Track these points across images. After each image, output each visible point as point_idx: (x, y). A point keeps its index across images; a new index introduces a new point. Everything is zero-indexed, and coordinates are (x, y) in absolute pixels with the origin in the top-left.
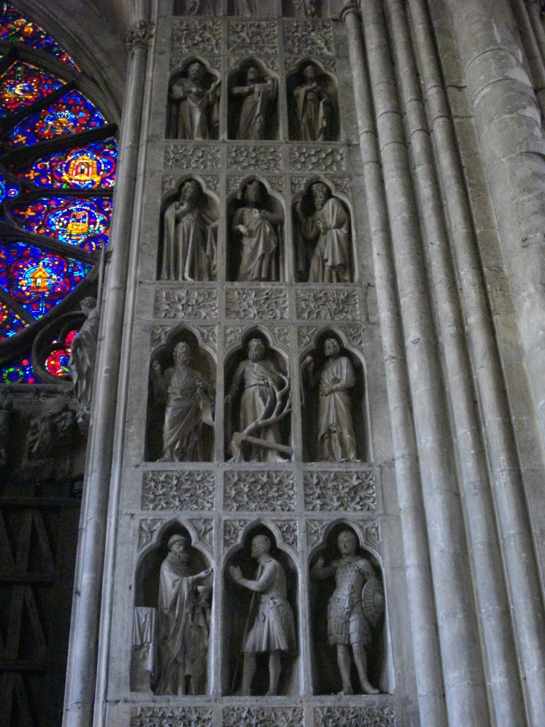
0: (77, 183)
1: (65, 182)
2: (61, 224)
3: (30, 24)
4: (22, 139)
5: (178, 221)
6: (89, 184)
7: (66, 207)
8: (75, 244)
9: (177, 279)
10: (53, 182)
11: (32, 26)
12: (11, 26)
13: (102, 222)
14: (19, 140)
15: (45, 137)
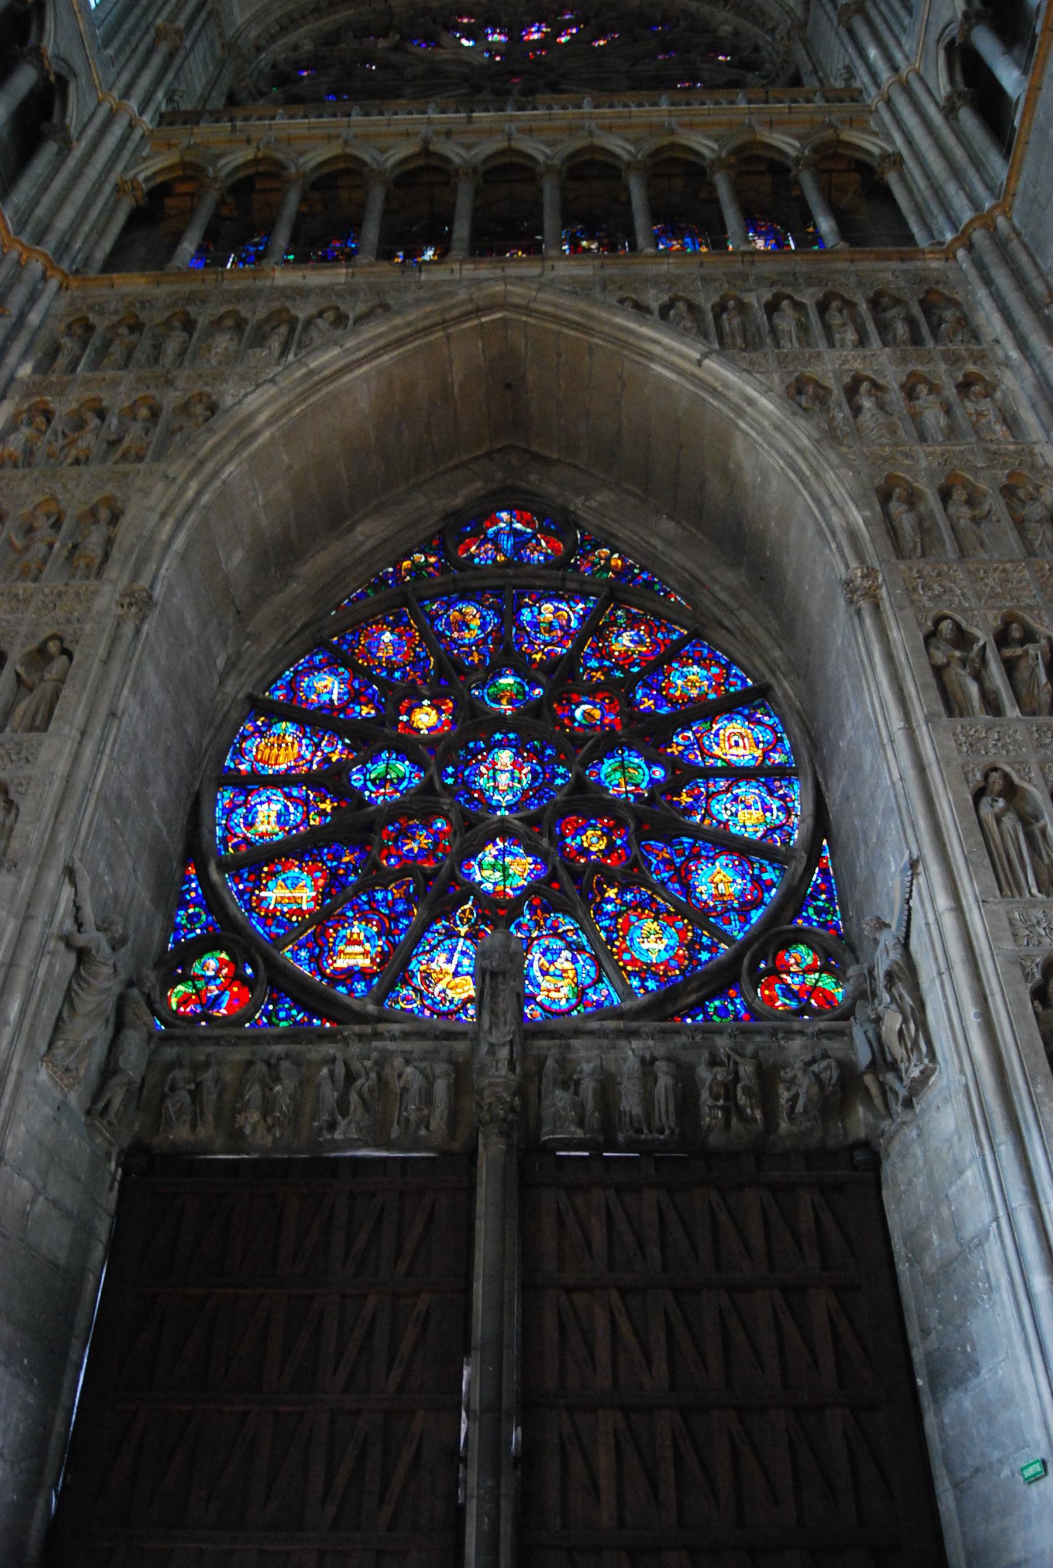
0: (734, 758)
1: (718, 757)
3: (616, 556)
4: (649, 703)
5: (998, 821)
7: (728, 790)
9: (1021, 895)
10: (703, 759)
12: (591, 558)
13: (778, 809)
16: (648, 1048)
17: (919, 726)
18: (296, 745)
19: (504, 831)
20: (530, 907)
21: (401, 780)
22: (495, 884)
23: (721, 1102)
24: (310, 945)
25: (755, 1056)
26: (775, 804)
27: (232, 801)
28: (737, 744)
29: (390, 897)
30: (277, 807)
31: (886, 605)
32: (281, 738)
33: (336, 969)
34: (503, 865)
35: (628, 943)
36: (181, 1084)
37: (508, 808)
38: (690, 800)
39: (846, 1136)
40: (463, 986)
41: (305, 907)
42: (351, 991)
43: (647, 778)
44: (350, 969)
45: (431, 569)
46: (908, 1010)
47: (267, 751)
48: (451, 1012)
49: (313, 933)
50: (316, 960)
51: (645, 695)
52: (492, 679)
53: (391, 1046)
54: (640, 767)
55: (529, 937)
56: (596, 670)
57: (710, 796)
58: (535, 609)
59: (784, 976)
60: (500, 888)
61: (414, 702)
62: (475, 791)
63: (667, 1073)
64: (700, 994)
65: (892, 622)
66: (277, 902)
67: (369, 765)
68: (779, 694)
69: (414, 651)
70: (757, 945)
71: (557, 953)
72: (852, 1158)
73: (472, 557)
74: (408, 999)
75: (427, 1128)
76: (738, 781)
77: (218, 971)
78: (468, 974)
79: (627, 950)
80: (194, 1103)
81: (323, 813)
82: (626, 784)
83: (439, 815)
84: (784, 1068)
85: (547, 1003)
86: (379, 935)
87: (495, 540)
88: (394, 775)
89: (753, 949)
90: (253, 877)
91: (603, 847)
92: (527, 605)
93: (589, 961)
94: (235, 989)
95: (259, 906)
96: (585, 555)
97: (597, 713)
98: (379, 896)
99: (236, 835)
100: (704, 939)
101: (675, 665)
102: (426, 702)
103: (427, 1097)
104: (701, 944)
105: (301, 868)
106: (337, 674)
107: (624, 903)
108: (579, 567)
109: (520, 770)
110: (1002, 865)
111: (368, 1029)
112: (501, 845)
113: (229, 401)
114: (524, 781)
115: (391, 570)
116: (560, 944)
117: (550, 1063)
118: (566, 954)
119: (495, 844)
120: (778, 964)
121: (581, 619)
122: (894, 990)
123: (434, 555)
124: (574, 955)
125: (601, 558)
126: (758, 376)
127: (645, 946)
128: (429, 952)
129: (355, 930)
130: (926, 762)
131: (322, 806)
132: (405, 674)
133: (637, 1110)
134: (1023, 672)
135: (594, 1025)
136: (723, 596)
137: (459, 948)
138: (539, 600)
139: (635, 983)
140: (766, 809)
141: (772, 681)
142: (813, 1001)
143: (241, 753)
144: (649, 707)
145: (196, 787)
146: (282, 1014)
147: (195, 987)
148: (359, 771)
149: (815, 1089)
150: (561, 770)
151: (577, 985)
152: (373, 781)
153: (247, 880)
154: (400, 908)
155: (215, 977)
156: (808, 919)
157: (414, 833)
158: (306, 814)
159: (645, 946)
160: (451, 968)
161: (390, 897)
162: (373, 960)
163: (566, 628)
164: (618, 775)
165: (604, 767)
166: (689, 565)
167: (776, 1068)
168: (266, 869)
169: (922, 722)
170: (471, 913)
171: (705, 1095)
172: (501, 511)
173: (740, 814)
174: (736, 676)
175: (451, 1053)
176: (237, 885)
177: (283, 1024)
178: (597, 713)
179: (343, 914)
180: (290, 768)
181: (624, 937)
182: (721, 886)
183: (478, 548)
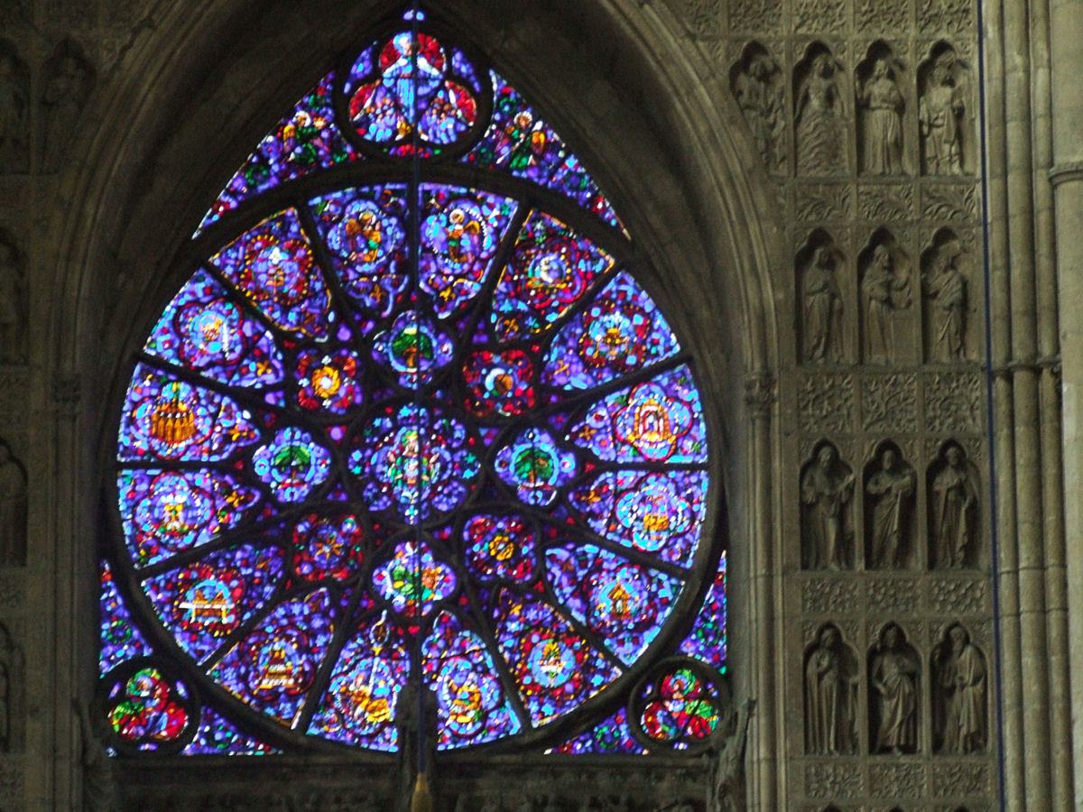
1: (632, 445)
2: (635, 516)
3: (539, 125)
5: (820, 677)
7: (636, 488)
11: (543, 130)
17: (777, 575)
19: (412, 536)
25: (630, 803)
31: (776, 422)
32: (173, 405)
33: (262, 690)
40: (380, 710)
47: (161, 422)
49: (238, 651)
57: (618, 495)
58: (443, 217)
65: (777, 455)
66: (197, 616)
73: (366, 122)
74: (330, 723)
77: (153, 690)
79: (529, 672)
81: (230, 508)
86: (300, 651)
92: (436, 213)
98: (296, 609)
102: (326, 360)
105: (217, 577)
107: (527, 622)
109: (430, 456)
110: (813, 724)
113: (105, 61)
118: (472, 675)
122: (726, 800)
126: (701, 44)
128: (346, 673)
129: (277, 647)
130: (776, 615)
134: (881, 512)
136: (655, 220)
137: (374, 670)
141: (696, 356)
147: (132, 708)
150: (471, 459)
152: (278, 467)
153: (165, 588)
154: (317, 623)
155: (151, 698)
159: (545, 669)
160: (368, 690)
169: (780, 572)
170: (384, 631)
173: (646, 518)
178: (509, 380)
182: (619, 604)
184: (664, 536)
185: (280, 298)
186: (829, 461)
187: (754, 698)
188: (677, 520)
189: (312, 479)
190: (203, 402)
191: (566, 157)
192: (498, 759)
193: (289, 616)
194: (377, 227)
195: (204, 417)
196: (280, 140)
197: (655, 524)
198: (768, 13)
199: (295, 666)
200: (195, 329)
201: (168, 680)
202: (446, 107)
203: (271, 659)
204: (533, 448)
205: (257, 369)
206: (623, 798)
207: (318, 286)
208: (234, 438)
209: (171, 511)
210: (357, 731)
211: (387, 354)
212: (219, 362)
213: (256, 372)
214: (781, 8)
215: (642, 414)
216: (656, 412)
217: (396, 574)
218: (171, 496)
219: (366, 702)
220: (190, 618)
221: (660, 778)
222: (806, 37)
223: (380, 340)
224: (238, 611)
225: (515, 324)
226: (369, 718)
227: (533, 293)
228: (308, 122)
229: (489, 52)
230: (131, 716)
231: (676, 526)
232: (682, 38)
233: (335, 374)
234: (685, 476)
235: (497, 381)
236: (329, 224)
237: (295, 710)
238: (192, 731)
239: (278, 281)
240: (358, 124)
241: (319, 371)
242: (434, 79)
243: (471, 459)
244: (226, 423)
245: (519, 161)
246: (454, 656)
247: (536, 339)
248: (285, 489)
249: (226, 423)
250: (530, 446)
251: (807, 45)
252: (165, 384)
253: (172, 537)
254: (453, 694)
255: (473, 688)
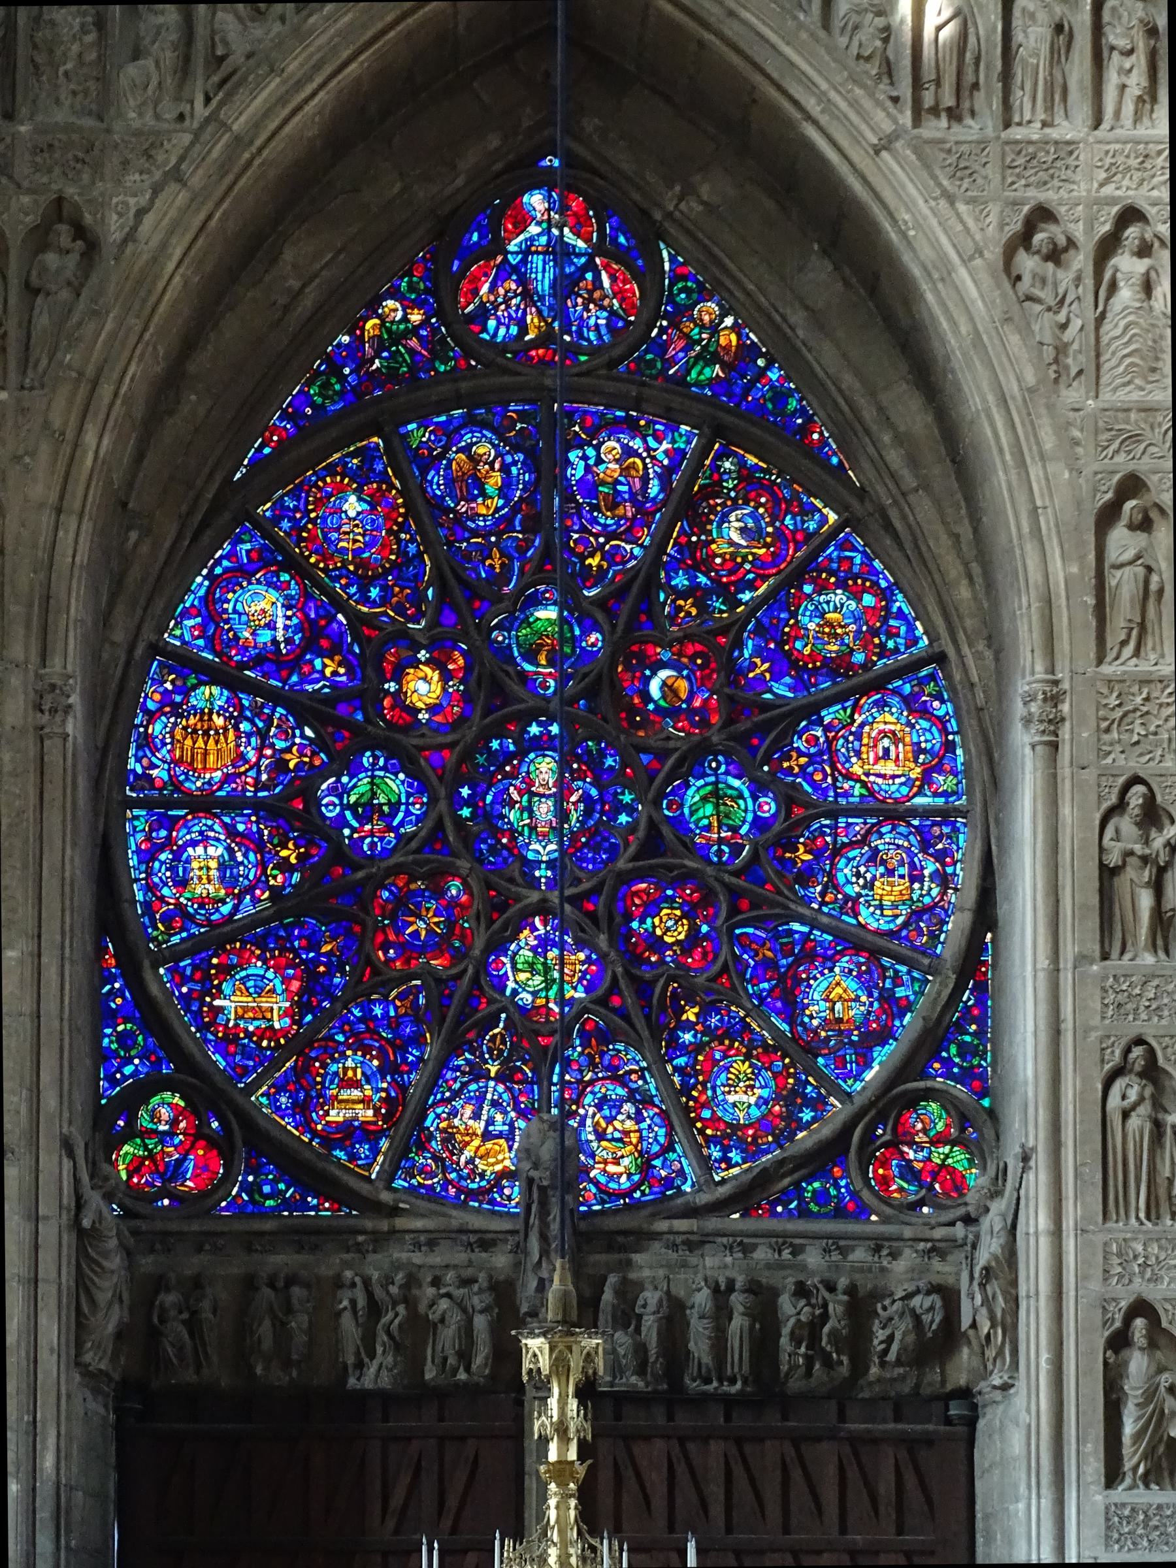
1: (858, 780)
2: (861, 881)
3: (729, 321)
5: (1126, 1115)
6: (902, 784)
7: (864, 841)
8: (892, 926)
10: (835, 780)
11: (735, 328)
13: (932, 877)
14: (758, 671)
15: (806, 664)
16: (725, 1267)
18: (231, 735)
19: (543, 909)
20: (583, 1034)
21: (395, 807)
22: (535, 994)
23: (803, 1350)
24: (291, 1087)
25: (852, 1290)
26: (930, 867)
27: (149, 838)
28: (886, 751)
29: (392, 1013)
30: (217, 851)
34: (545, 964)
35: (709, 1093)
36: (173, 1313)
37: (551, 864)
38: (808, 857)
39: (943, 1382)
41: (277, 1026)
42: (353, 1157)
43: (750, 817)
44: (348, 1123)
45: (414, 343)
46: (999, 1315)
47: (189, 742)
48: (482, 1191)
49: (293, 1068)
50: (303, 1110)
51: (758, 652)
52: (522, 610)
53: (417, 1258)
54: (741, 796)
55: (580, 1081)
56: (683, 594)
57: (838, 851)
59: (906, 1149)
60: (540, 1002)
61: (405, 653)
62: (503, 833)
63: (744, 1314)
64: (796, 1176)
67: (345, 779)
68: (958, 677)
69: (399, 541)
70: (873, 1112)
71: (617, 1105)
72: (947, 1409)
73: (483, 313)
74: (424, 1171)
75: (468, 1369)
76: (880, 824)
77: (174, 1123)
78: (500, 1135)
80: (192, 1335)
81: (285, 866)
82: (720, 827)
83: (455, 875)
84: (883, 1297)
85: (602, 1180)
86: (382, 1071)
87: (520, 273)
88: (383, 801)
89: (866, 1119)
90: (198, 975)
91: (682, 937)
92: (581, 445)
93: (657, 1120)
94: (201, 1152)
95: (213, 1023)
96: (675, 324)
97: (683, 686)
98: (378, 1011)
99: (162, 899)
100: (809, 1089)
101: (808, 589)
102: (423, 655)
103: (467, 1329)
104: (804, 1096)
106: (280, 587)
107: (707, 1031)
108: (665, 346)
111: (384, 1225)
112: (542, 931)
113: (114, 228)
114: (574, 816)
115: (346, 339)
116: (621, 1091)
117: (608, 1296)
118: (628, 1107)
119: (534, 929)
120: (900, 1129)
121: (665, 477)
122: (988, 1287)
123: (418, 304)
124: (638, 1112)
125: (703, 327)
126: (962, 207)
127: (731, 1098)
129: (350, 1063)
131: (284, 853)
132: (386, 591)
133: (707, 1360)
135: (662, 1225)
136: (894, 457)
137: (489, 1096)
138: (597, 430)
139: (716, 1154)
140: (916, 876)
142: (937, 1186)
143: (148, 743)
144: (760, 679)
145: (101, 828)
146: (267, 1189)
148: (331, 791)
149: (911, 1338)
151: (641, 1153)
155: (171, 1134)
156: (948, 1063)
157: (418, 906)
158: (262, 865)
159: (731, 1098)
160: (479, 1127)
161: (392, 1013)
162: (377, 1111)
163: (638, 499)
164: (709, 809)
165: (690, 792)
166: (848, 380)
167: (878, 1295)
168: (215, 961)
169: (1070, 965)
170: (504, 1042)
171: (784, 1341)
172: (530, 188)
174: (900, 615)
175: (491, 1277)
176: (179, 988)
177: (270, 1203)
178: (683, 686)
179: (330, 1038)
180: (227, 779)
181: (704, 1084)
182: (838, 1006)
183: (492, 290)
184: (904, 910)
185: (357, 569)
186: (1142, 806)
187: (1031, 1143)
188: (921, 889)
189: (401, 824)
190: (248, 713)
191: (769, 366)
192: (662, 1225)
193: (368, 1017)
194: (497, 466)
195: (249, 735)
196: (359, 341)
197: (890, 893)
198: (1058, 164)
199: (379, 1090)
200: (239, 607)
201: (194, 1109)
202: (597, 295)
203: (341, 1080)
204: (716, 783)
205: (325, 666)
206: (843, 1282)
207: (412, 548)
208: (292, 765)
209: (201, 869)
210: (463, 1183)
211: (509, 645)
212: (268, 659)
213: (322, 672)
214: (1077, 158)
215: (873, 734)
216: (893, 732)
217: (520, 960)
218: (200, 850)
219: (477, 1142)
220: (228, 1020)
221: (894, 1255)
222: (1112, 201)
223: (498, 627)
224: (294, 1013)
225: (693, 605)
226: (481, 1165)
227: (718, 561)
228: (400, 314)
229: (658, 216)
230: (144, 1158)
231: (922, 896)
232: (935, 199)
233: (436, 676)
234: (935, 824)
235: (664, 683)
236: (428, 462)
237: (375, 1151)
238: (228, 1179)
239: (355, 541)
240: (470, 319)
241: (411, 671)
242: (579, 255)
243: (627, 798)
244: (280, 745)
245: (700, 373)
246: (603, 1078)
247: (724, 630)
248: (362, 839)
249: (280, 745)
250: (712, 779)
251: (1115, 210)
252: (195, 688)
253: (202, 906)
254: (601, 1136)
255: (629, 1125)
